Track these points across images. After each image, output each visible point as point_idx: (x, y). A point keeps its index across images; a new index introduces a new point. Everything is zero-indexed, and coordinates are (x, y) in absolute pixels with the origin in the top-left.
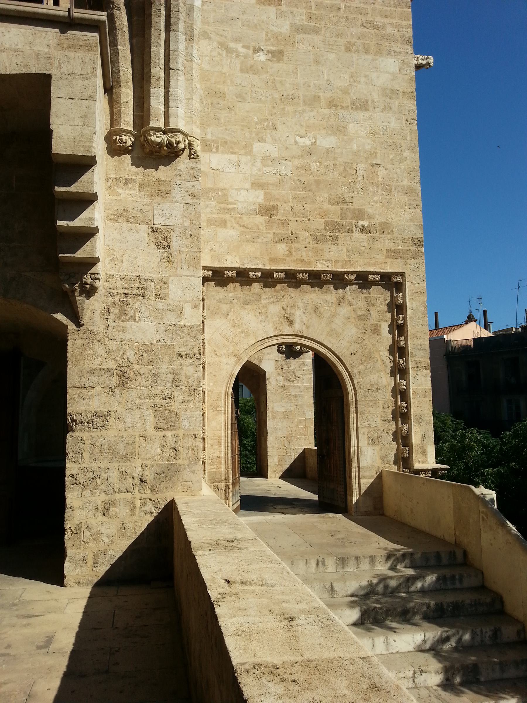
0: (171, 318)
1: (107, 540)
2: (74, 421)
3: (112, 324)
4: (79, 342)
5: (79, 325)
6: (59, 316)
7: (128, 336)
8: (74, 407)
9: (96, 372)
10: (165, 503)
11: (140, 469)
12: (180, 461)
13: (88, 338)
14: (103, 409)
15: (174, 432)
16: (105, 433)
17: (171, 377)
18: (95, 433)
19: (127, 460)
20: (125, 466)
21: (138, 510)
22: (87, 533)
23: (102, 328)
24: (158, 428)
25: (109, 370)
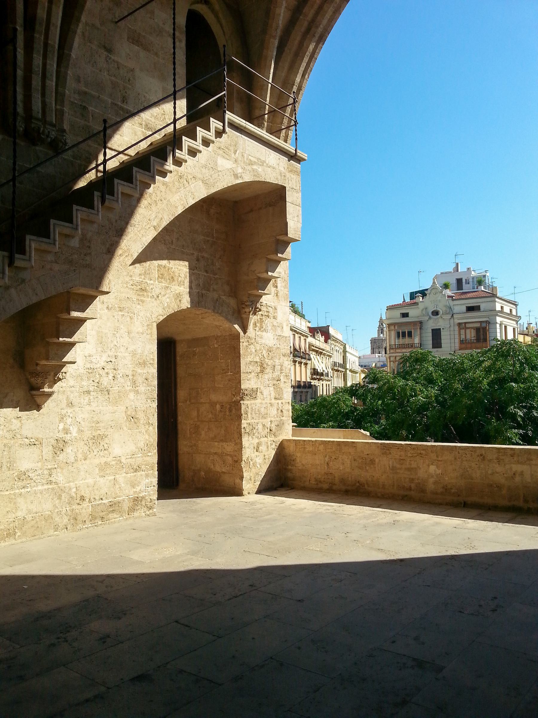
0: (279, 332)
1: (259, 466)
2: (244, 394)
3: (257, 333)
4: (245, 344)
5: (245, 332)
6: (236, 326)
7: (263, 341)
8: (244, 385)
9: (252, 363)
10: (279, 443)
11: (270, 423)
12: (284, 418)
13: (248, 341)
14: (255, 387)
15: (281, 401)
16: (256, 401)
17: (279, 367)
18: (253, 402)
19: (265, 418)
20: (264, 421)
21: (270, 447)
22: (251, 463)
23: (254, 334)
24: (275, 399)
25: (257, 362)
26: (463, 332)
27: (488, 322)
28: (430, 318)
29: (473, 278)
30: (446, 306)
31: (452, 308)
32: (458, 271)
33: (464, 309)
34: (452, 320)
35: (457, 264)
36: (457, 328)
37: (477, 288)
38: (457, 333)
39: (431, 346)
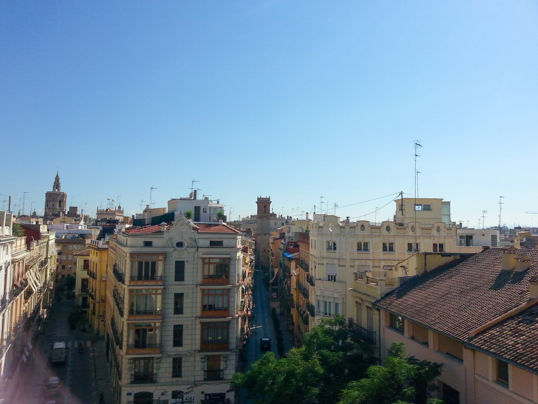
26: (206, 266)
27: (230, 259)
28: (175, 250)
29: (210, 208)
30: (191, 238)
31: (197, 240)
32: (195, 198)
33: (208, 244)
34: (196, 254)
35: (195, 191)
36: (200, 261)
37: (218, 221)
38: (200, 266)
39: (173, 278)
